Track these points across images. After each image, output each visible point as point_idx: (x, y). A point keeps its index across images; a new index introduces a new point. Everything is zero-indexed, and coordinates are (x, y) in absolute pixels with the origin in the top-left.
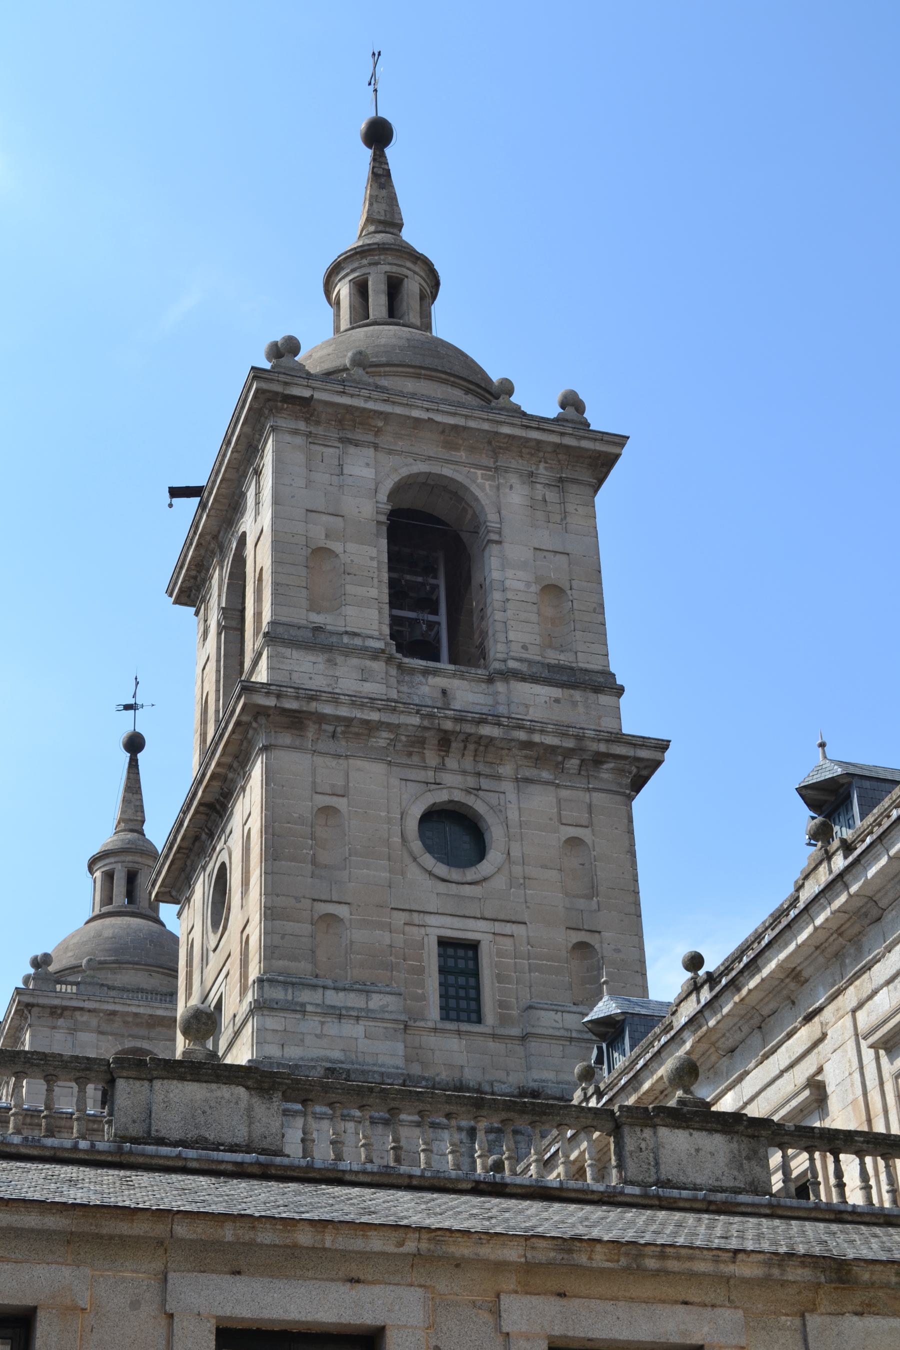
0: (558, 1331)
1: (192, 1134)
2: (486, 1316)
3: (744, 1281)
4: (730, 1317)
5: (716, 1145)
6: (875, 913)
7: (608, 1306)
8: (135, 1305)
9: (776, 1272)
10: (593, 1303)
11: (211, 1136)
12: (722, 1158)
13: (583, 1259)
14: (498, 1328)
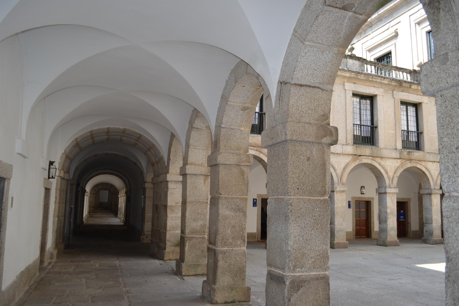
0: (354, 90)
2: (342, 86)
3: (385, 84)
4: (381, 90)
5: (357, 62)
6: (371, 25)
7: (362, 86)
9: (390, 83)
10: (360, 85)
12: (358, 65)
13: (359, 77)
14: (344, 88)
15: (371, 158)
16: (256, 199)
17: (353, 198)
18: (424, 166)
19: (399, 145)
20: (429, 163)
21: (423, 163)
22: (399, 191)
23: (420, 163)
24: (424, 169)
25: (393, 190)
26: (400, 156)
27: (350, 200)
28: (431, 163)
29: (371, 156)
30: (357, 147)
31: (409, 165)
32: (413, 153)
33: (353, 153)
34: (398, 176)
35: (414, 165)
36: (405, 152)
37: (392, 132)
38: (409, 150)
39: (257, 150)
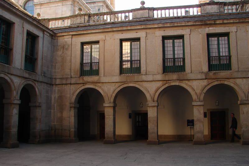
0: (163, 35)
1: (141, 17)
8: (110, 39)
11: (144, 17)
15: (178, 81)
16: (131, 114)
17: (208, 110)
18: (232, 83)
19: (205, 68)
20: (238, 79)
21: (232, 80)
22: (192, 103)
23: (228, 80)
24: (232, 85)
25: (199, 103)
26: (206, 76)
27: (206, 111)
28: (241, 79)
29: (178, 80)
30: (165, 75)
31: (216, 83)
32: (219, 73)
33: (162, 80)
34: (205, 92)
35: (222, 82)
36: (211, 74)
37: (199, 59)
38: (214, 72)
39: (93, 85)
